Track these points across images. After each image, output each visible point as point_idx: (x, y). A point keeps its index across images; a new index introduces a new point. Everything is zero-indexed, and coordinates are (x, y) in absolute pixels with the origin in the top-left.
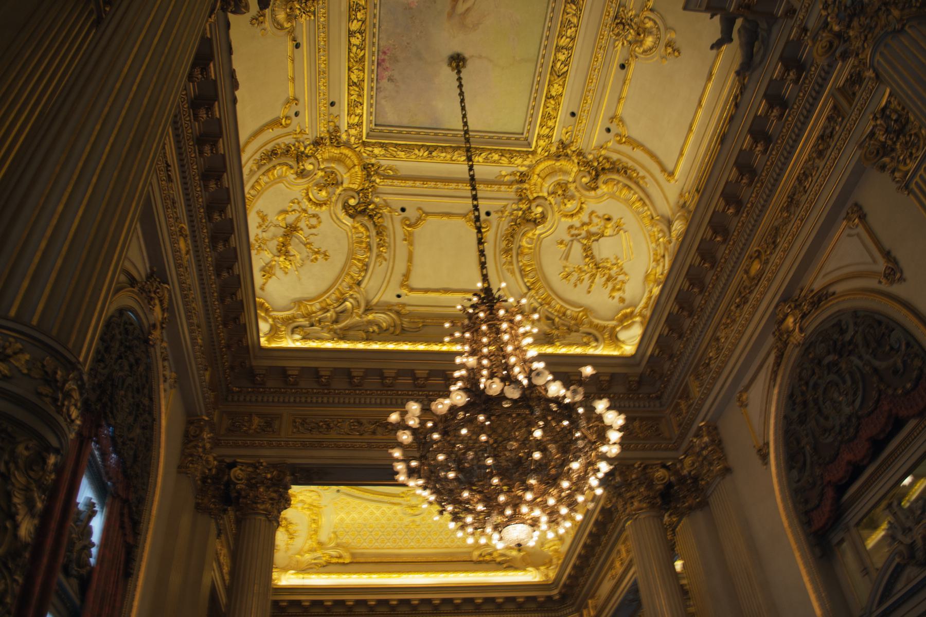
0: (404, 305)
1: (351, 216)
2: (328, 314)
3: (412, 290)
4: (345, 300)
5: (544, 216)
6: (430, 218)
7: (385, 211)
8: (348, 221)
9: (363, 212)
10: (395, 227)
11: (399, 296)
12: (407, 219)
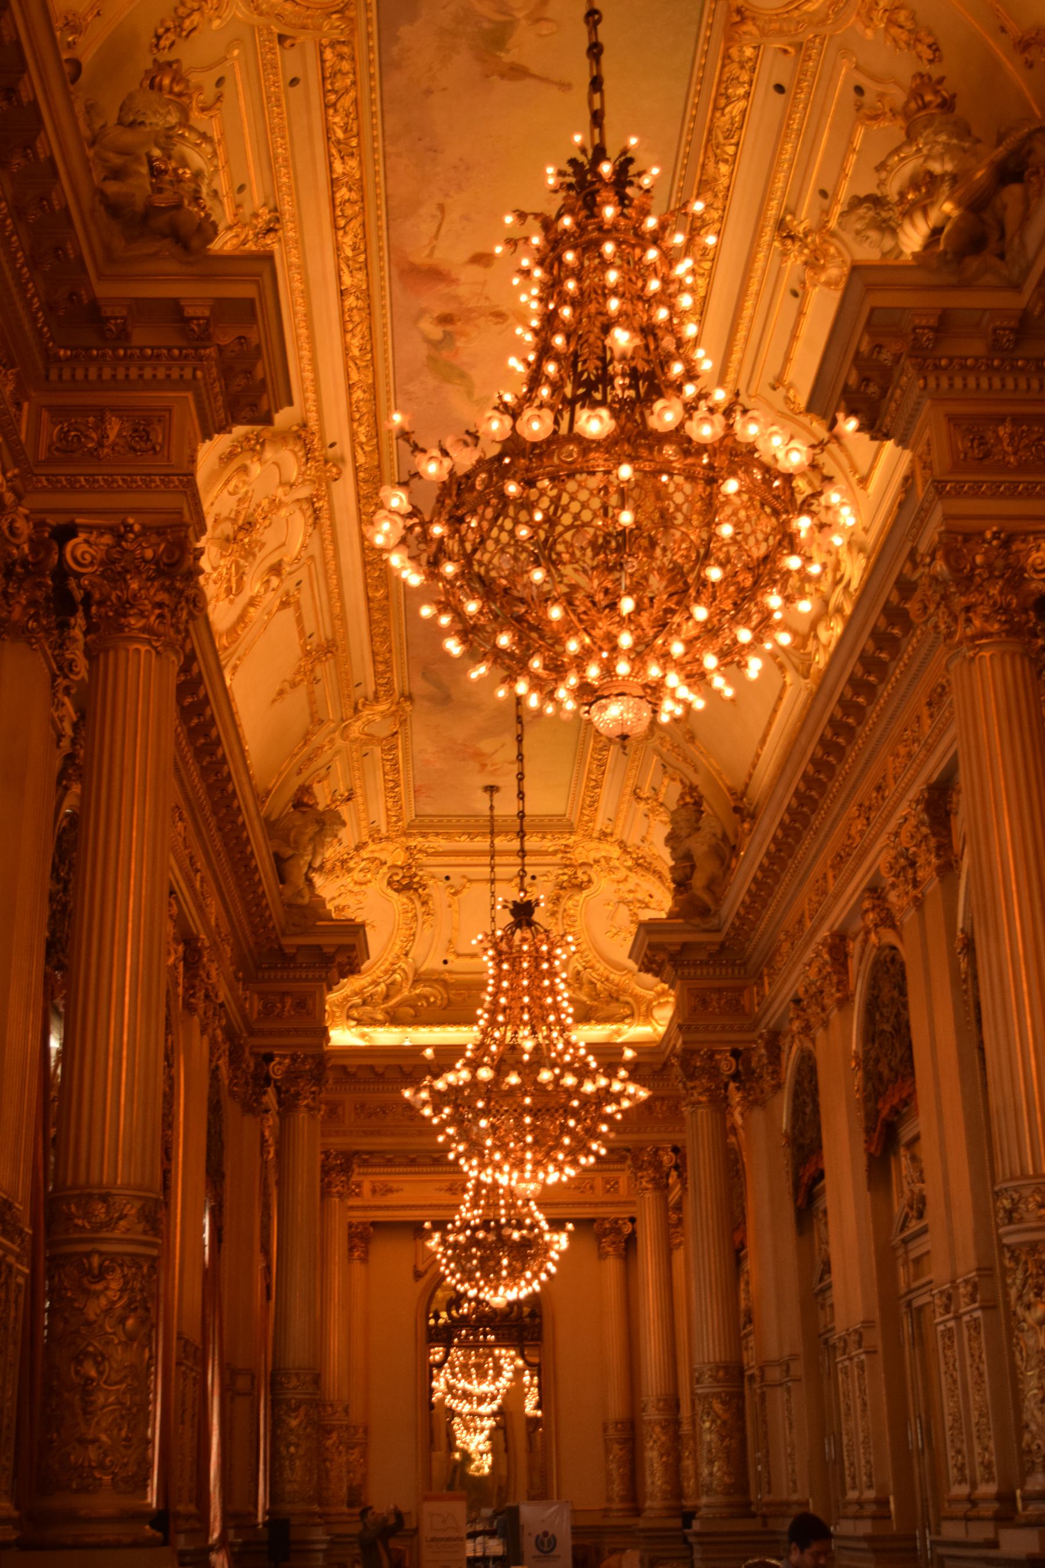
0: (450, 972)
1: (396, 890)
2: (379, 989)
3: (459, 955)
4: (394, 972)
5: (590, 881)
6: (475, 885)
7: (431, 882)
8: (395, 895)
9: (408, 887)
10: (438, 892)
11: (445, 962)
12: (452, 886)
